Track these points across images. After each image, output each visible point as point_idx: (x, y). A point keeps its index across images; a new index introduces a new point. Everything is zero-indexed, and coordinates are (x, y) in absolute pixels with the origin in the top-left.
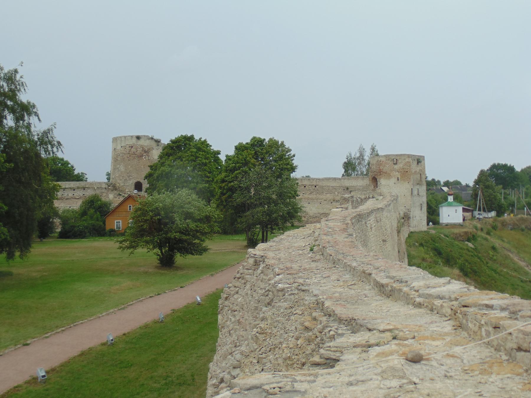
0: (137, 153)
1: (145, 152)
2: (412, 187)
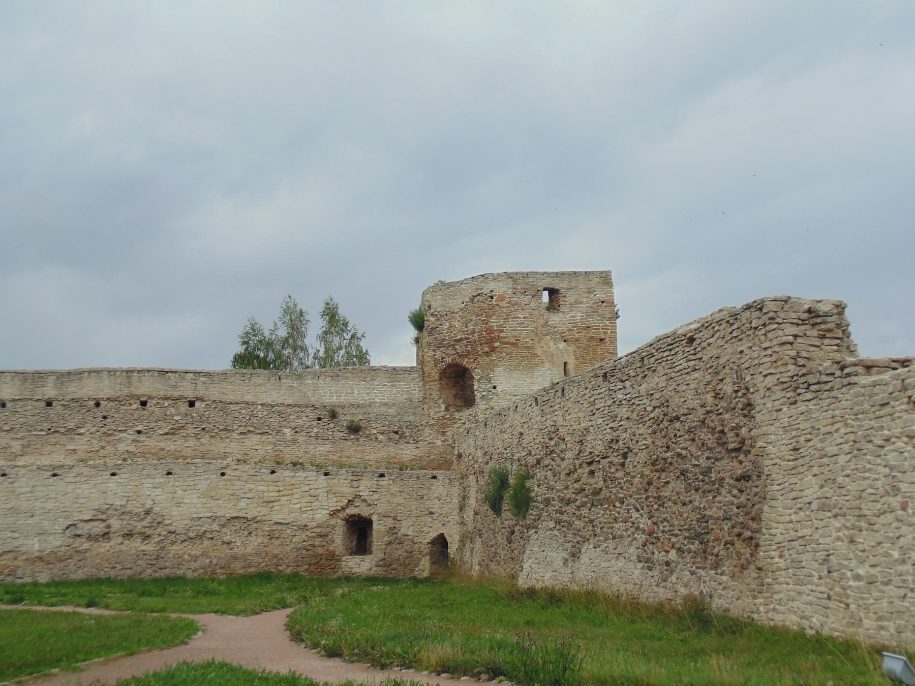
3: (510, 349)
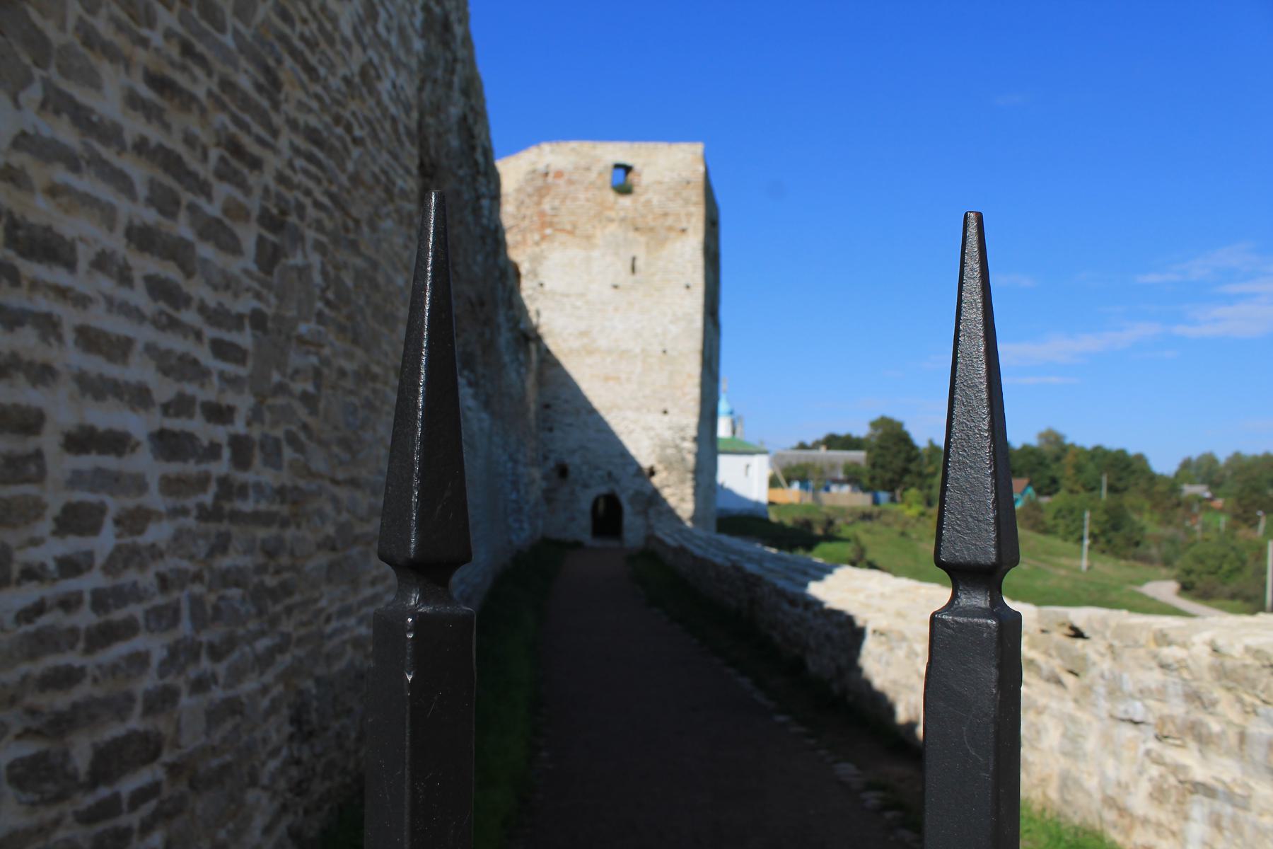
3: (561, 237)
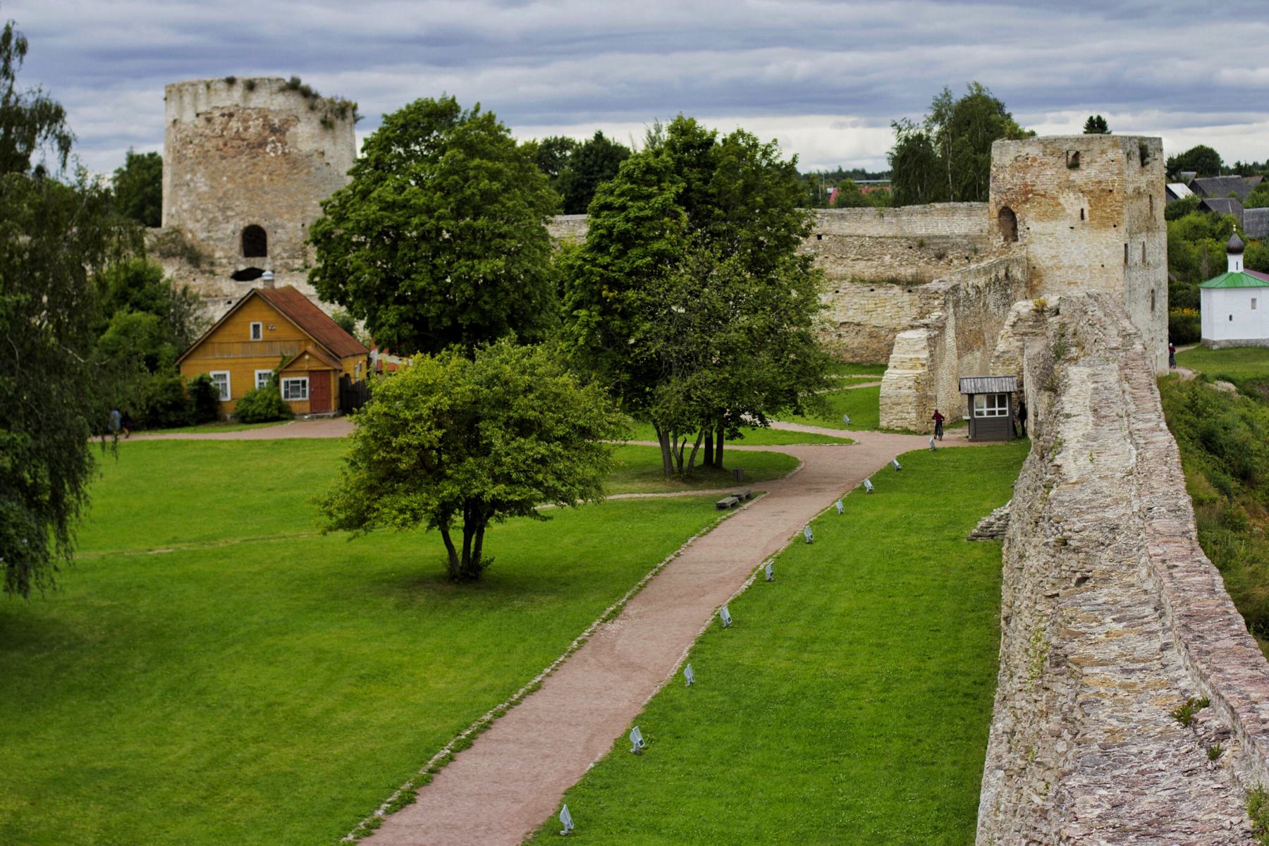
0: (246, 135)
1: (274, 130)
2: (1127, 241)
3: (1039, 199)
